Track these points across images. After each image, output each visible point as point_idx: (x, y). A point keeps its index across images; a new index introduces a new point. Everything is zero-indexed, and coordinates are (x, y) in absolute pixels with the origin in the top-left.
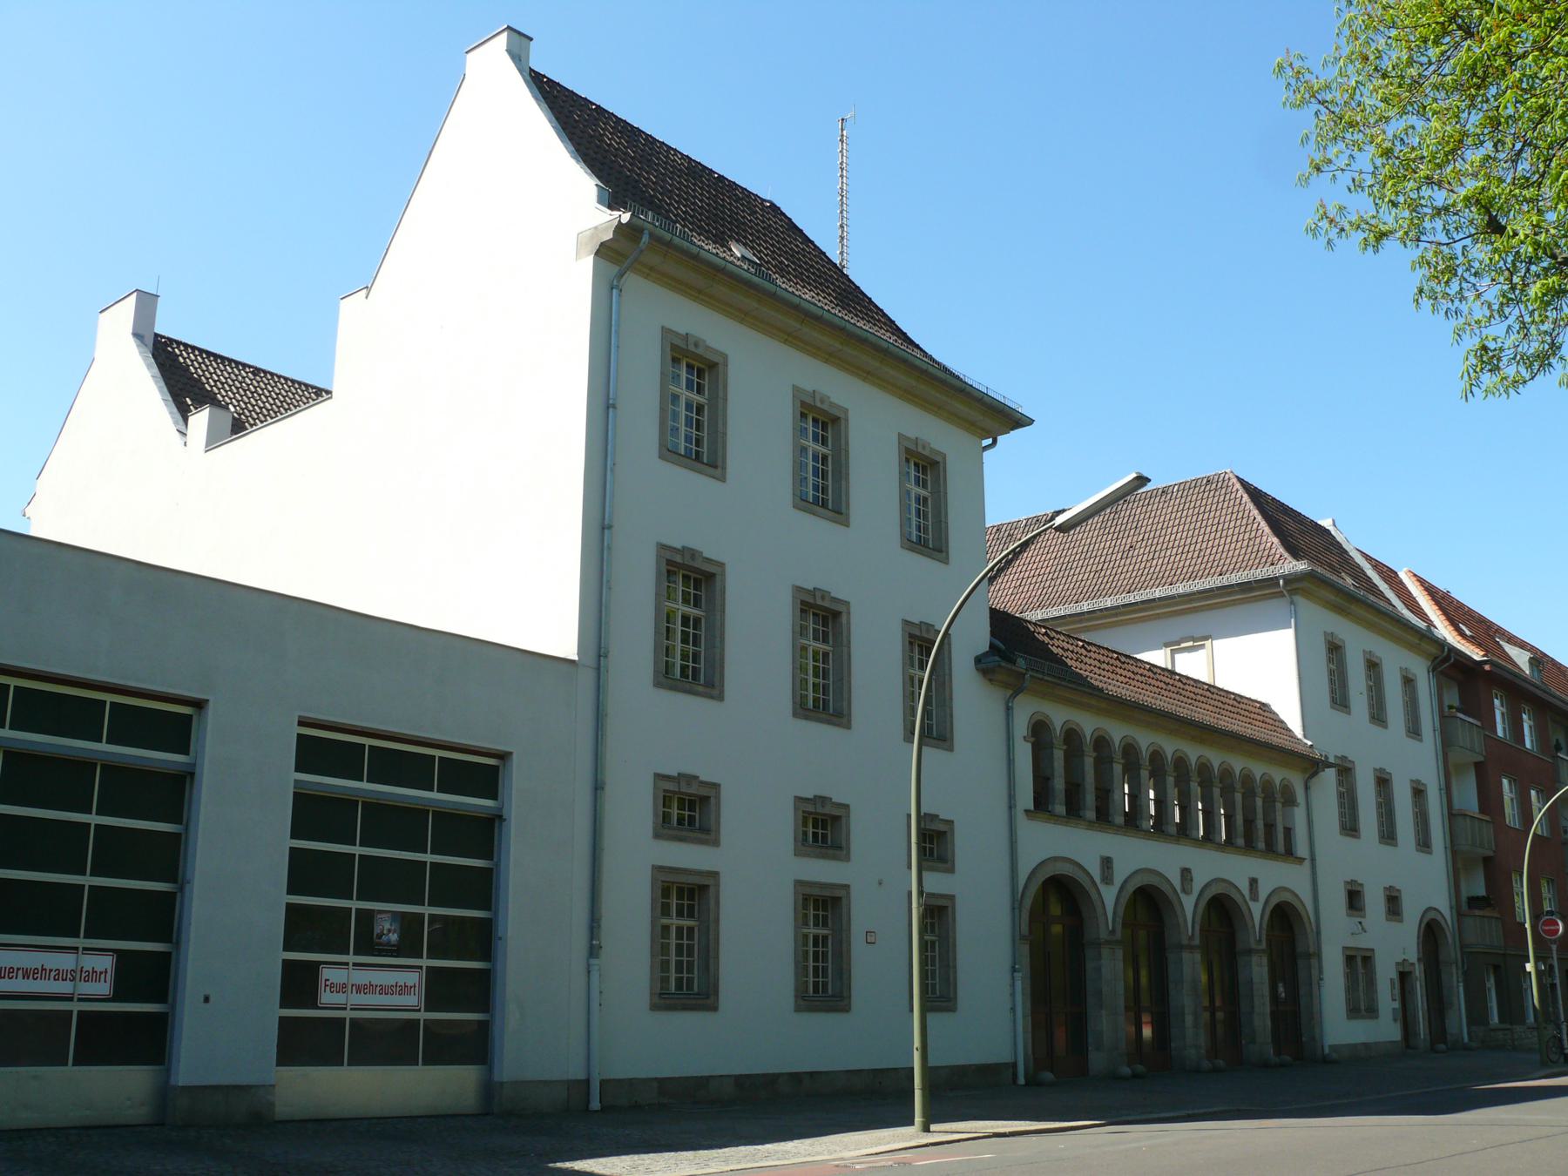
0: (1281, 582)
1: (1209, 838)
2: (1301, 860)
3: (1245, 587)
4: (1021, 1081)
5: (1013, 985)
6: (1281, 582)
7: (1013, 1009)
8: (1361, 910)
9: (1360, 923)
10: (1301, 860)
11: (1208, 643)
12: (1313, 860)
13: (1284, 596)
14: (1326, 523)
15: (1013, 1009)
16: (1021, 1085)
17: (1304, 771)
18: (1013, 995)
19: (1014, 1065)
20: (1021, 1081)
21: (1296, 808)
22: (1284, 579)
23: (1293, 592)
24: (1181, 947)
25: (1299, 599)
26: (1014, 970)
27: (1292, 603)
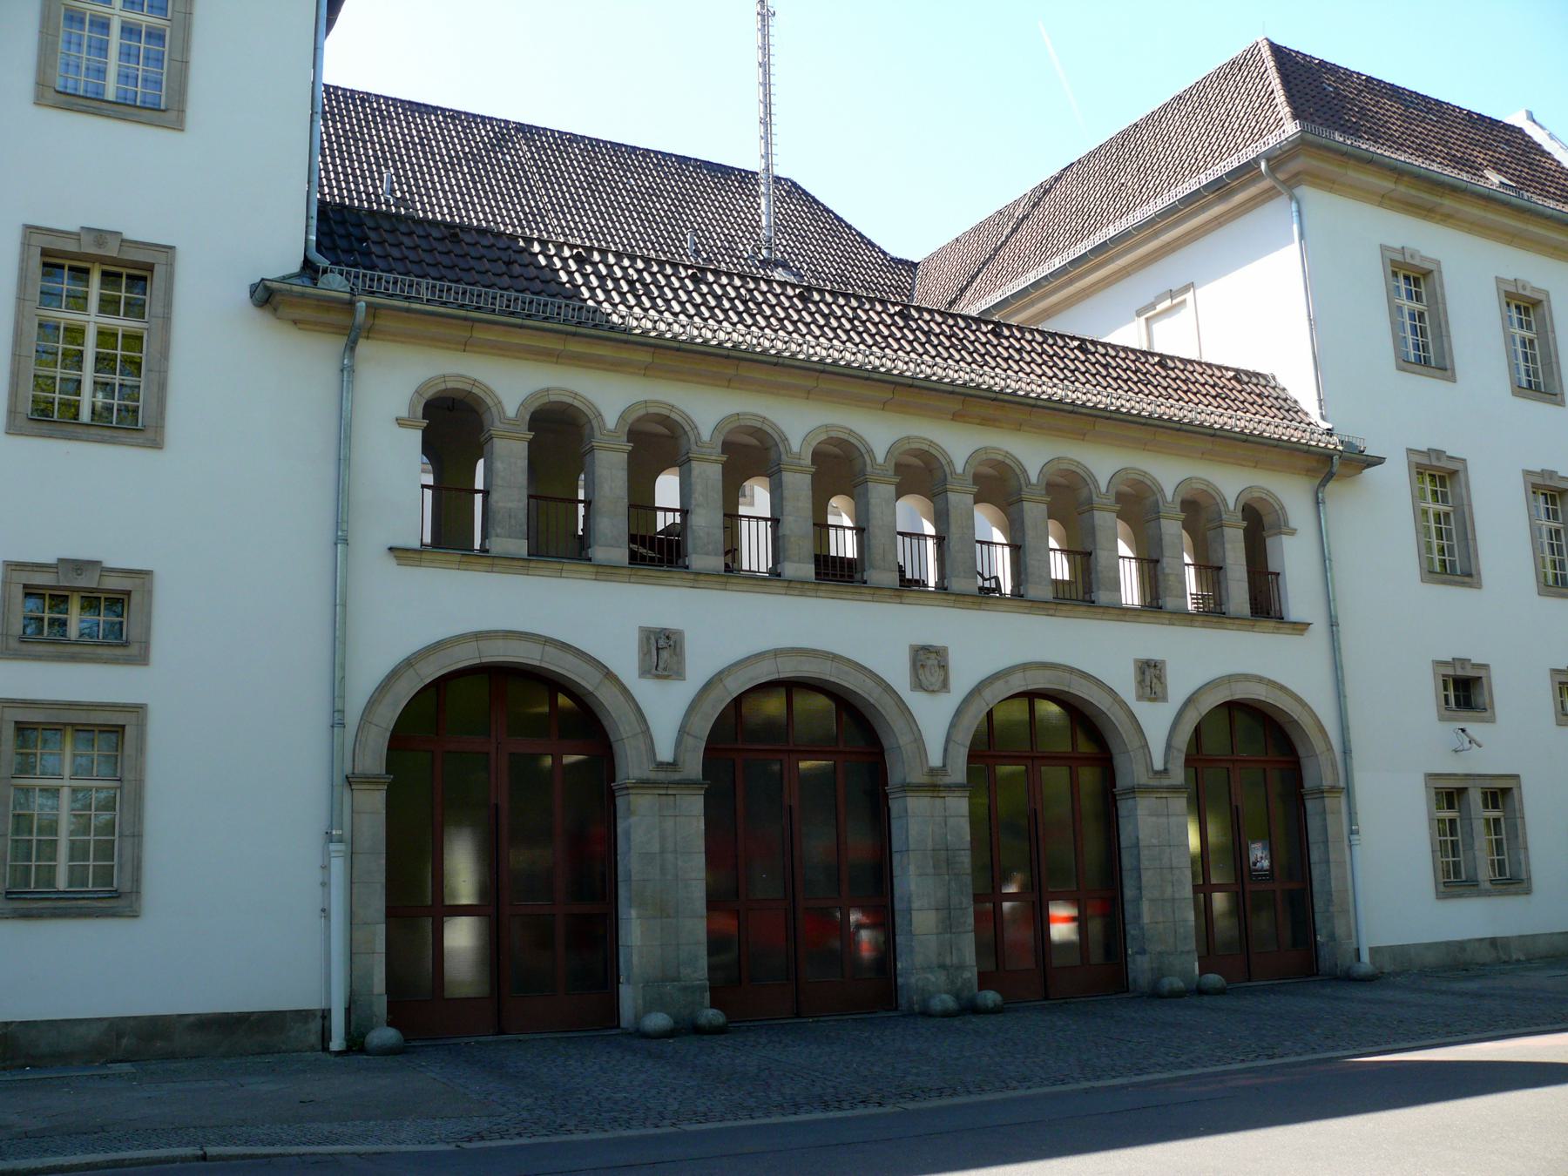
0: (1263, 165)
1: (1156, 602)
2: (1301, 627)
3: (1220, 188)
4: (337, 1043)
5: (325, 867)
6: (1263, 165)
7: (325, 912)
8: (1485, 709)
9: (1463, 730)
10: (1301, 627)
11: (1189, 296)
12: (1333, 624)
13: (1279, 194)
14: (1516, 119)
15: (325, 912)
16: (338, 1053)
17: (1309, 472)
18: (325, 884)
19: (326, 1015)
20: (337, 1043)
21: (1284, 537)
22: (1268, 160)
23: (1292, 183)
24: (907, 788)
25: (1306, 192)
26: (329, 838)
27: (1292, 197)
